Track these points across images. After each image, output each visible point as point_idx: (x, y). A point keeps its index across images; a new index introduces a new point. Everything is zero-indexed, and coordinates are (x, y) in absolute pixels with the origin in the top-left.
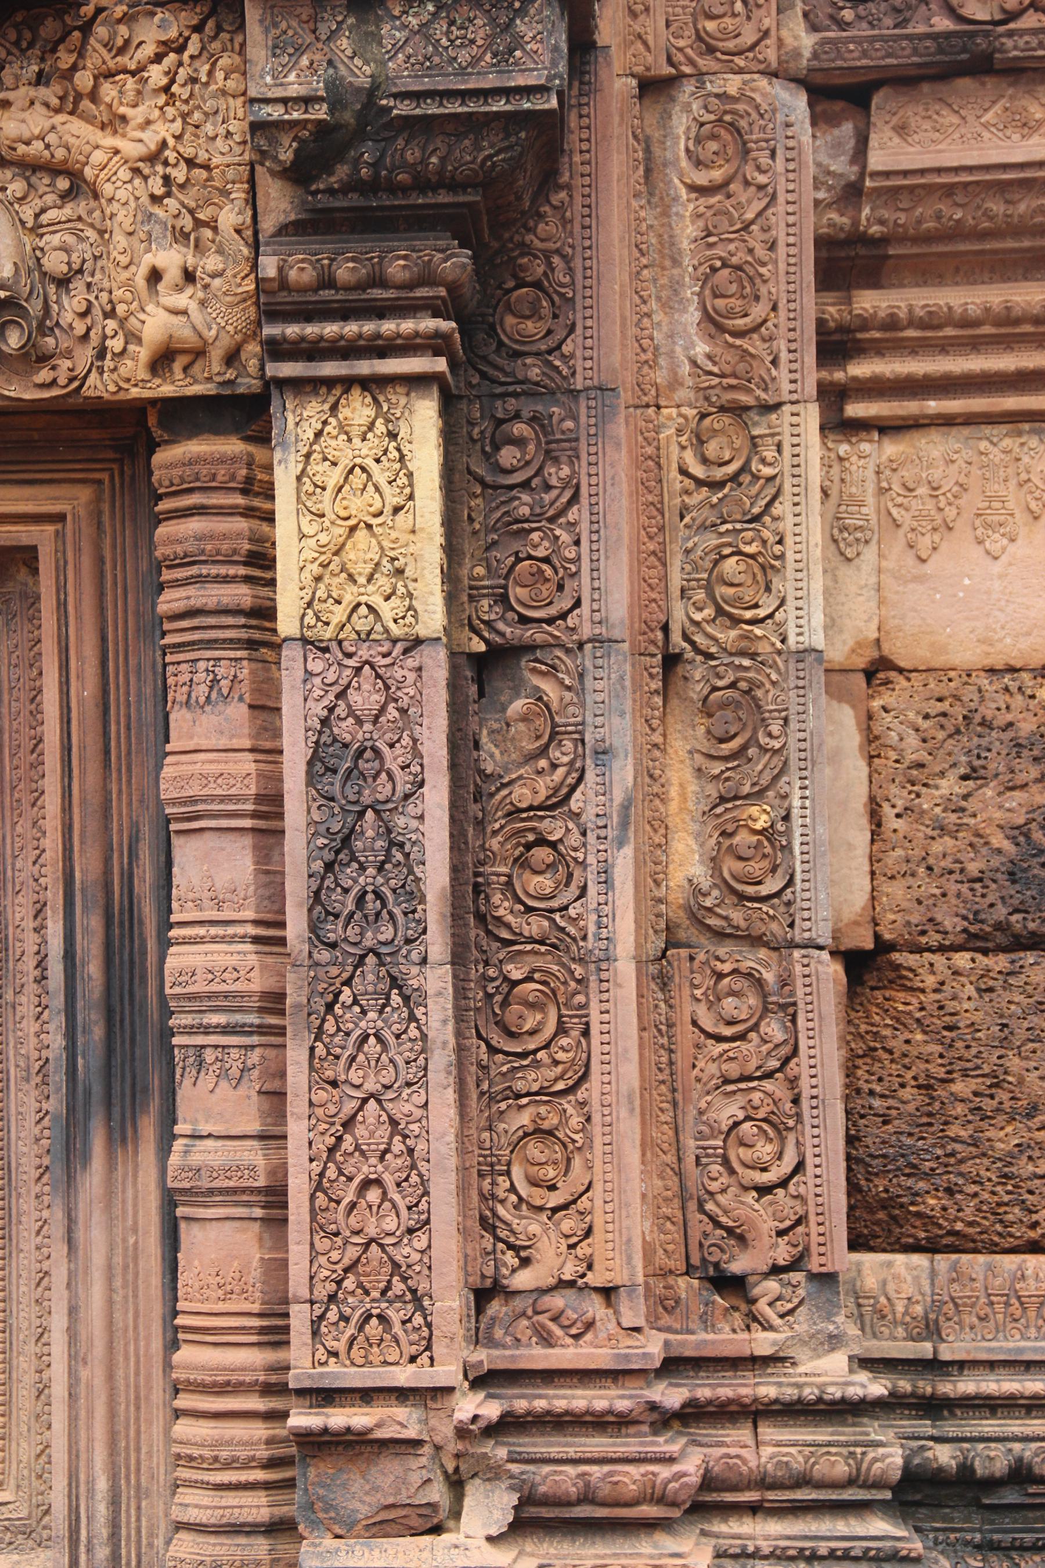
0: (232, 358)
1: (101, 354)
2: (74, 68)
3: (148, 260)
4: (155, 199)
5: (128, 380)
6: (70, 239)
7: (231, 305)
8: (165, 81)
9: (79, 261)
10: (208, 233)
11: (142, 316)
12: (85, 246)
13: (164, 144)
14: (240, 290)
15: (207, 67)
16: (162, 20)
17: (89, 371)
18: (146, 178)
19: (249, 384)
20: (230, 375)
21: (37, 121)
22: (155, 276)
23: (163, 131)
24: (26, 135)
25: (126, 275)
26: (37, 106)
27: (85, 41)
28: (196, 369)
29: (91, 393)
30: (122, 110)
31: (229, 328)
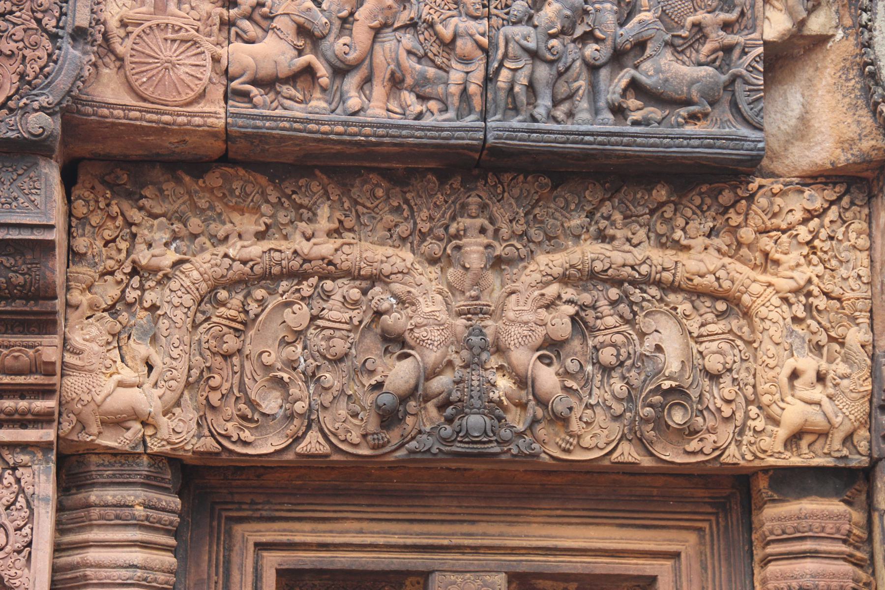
0: (848, 439)
1: (741, 433)
2: (738, 226)
3: (790, 364)
4: (796, 320)
5: (765, 452)
6: (725, 346)
7: (854, 400)
8: (810, 237)
9: (731, 362)
10: (837, 347)
11: (782, 405)
12: (736, 351)
13: (809, 281)
14: (862, 389)
15: (843, 229)
16: (811, 195)
17: (730, 443)
18: (790, 305)
19: (858, 461)
20: (845, 452)
21: (712, 261)
22: (795, 375)
23: (808, 272)
24: (703, 270)
25: (771, 374)
26: (711, 250)
27: (749, 208)
28: (817, 446)
29: (730, 460)
30: (777, 256)
31: (852, 417)
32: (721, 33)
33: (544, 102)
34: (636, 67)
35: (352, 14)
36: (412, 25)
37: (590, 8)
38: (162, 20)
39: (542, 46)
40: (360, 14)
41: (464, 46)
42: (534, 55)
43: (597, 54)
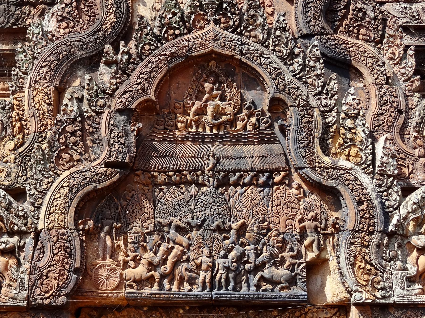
32: (291, 259)
33: (232, 284)
34: (263, 271)
35: (167, 257)
36: (188, 260)
37: (246, 252)
38: (104, 263)
39: (230, 265)
40: (170, 257)
41: (204, 267)
42: (228, 269)
43: (249, 268)
